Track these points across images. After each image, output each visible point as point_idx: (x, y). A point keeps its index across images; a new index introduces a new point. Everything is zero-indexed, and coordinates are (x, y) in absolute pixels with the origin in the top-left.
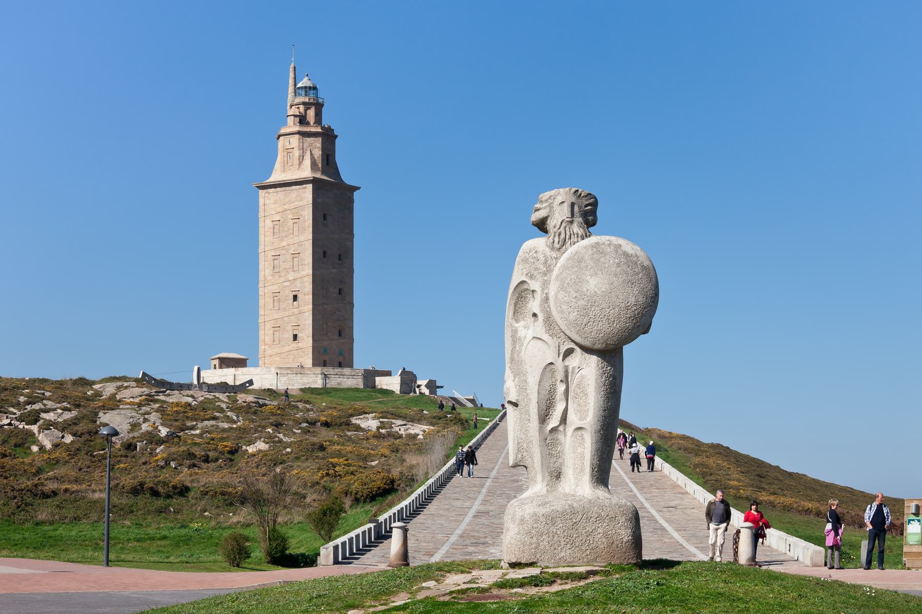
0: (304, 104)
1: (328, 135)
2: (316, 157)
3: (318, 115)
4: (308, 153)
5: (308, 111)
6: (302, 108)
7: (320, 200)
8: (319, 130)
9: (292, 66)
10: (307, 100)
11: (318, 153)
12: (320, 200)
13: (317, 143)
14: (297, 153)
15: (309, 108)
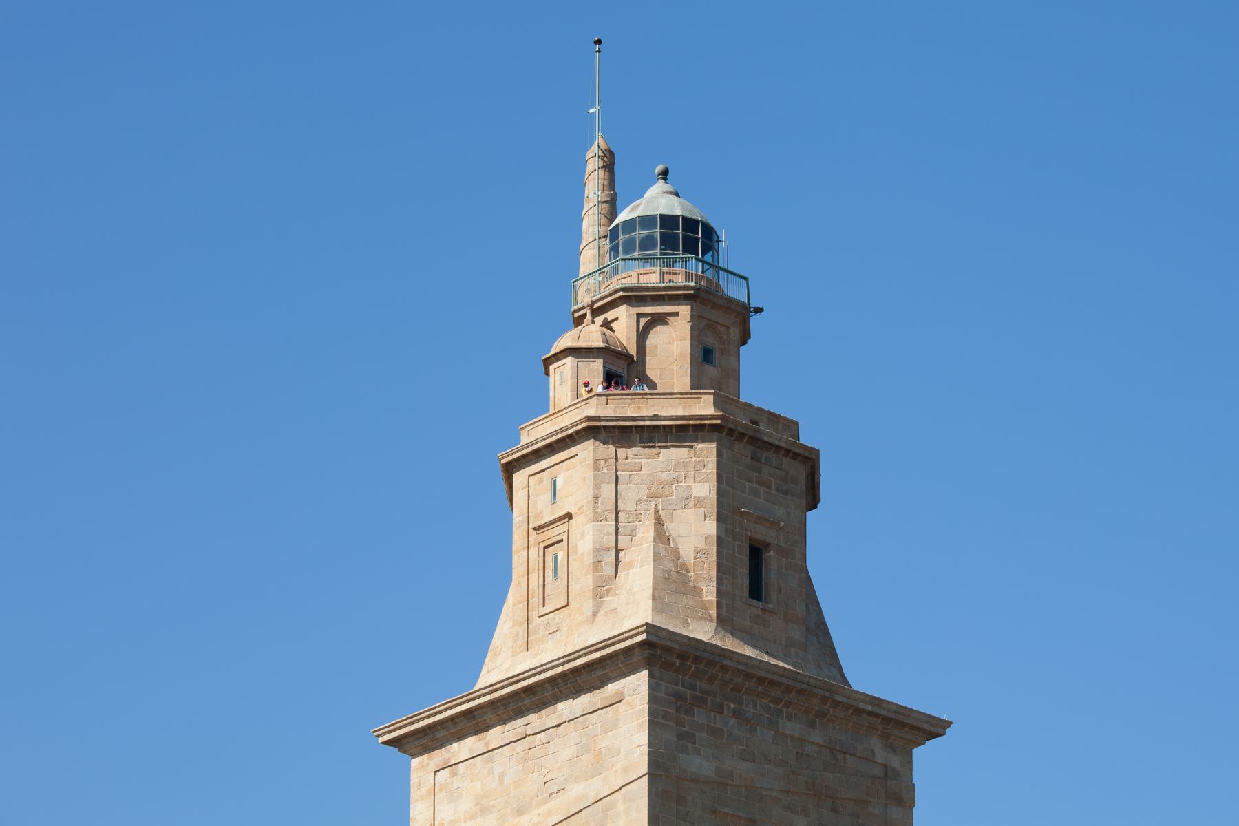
0: (633, 297)
1: (756, 441)
2: (687, 552)
3: (713, 357)
4: (646, 532)
5: (657, 337)
6: (624, 321)
7: (699, 764)
8: (705, 407)
9: (599, 142)
10: (651, 277)
11: (696, 531)
12: (699, 764)
13: (693, 474)
14: (585, 537)
15: (659, 319)
